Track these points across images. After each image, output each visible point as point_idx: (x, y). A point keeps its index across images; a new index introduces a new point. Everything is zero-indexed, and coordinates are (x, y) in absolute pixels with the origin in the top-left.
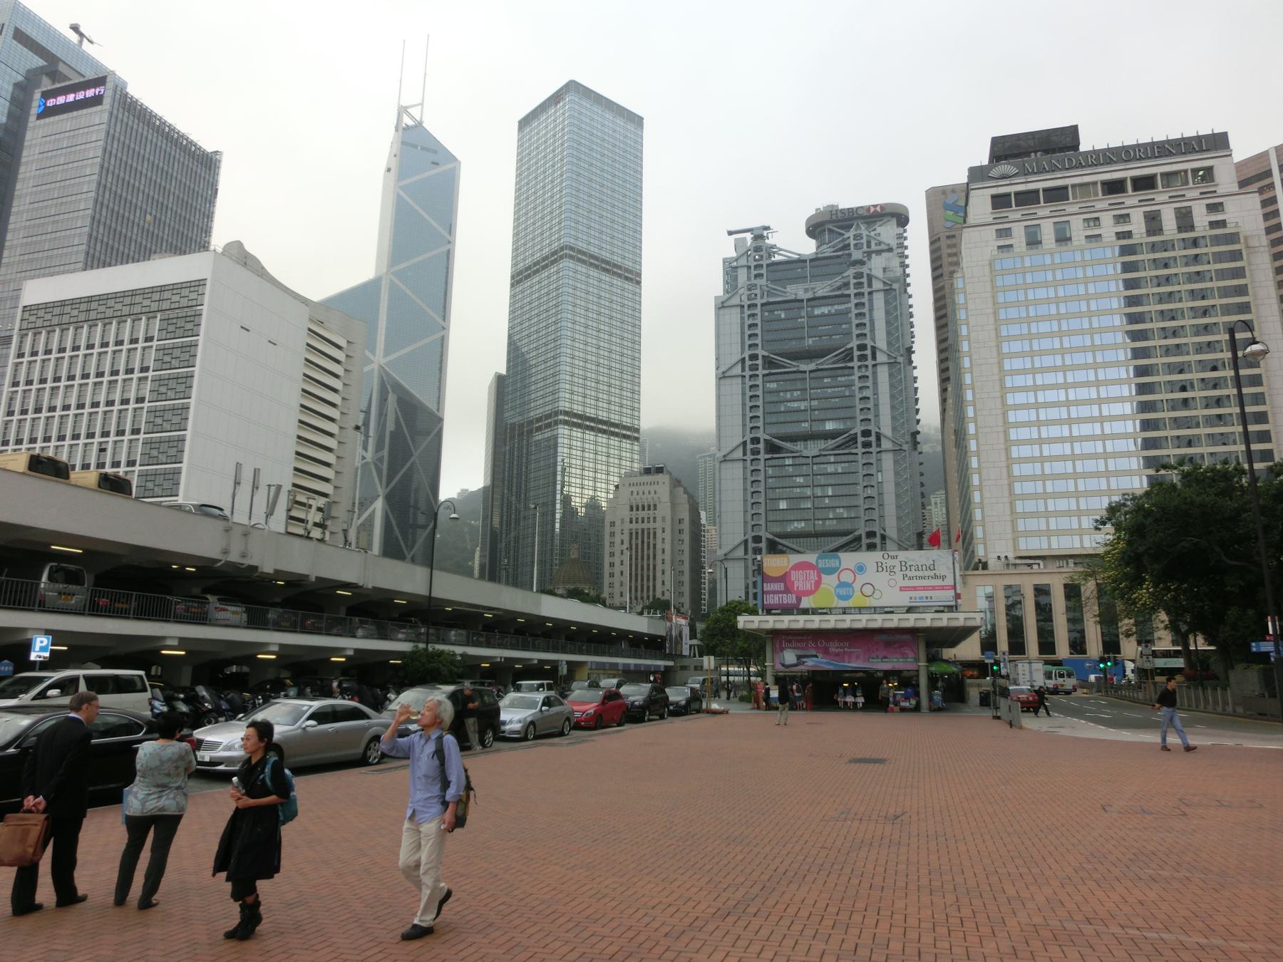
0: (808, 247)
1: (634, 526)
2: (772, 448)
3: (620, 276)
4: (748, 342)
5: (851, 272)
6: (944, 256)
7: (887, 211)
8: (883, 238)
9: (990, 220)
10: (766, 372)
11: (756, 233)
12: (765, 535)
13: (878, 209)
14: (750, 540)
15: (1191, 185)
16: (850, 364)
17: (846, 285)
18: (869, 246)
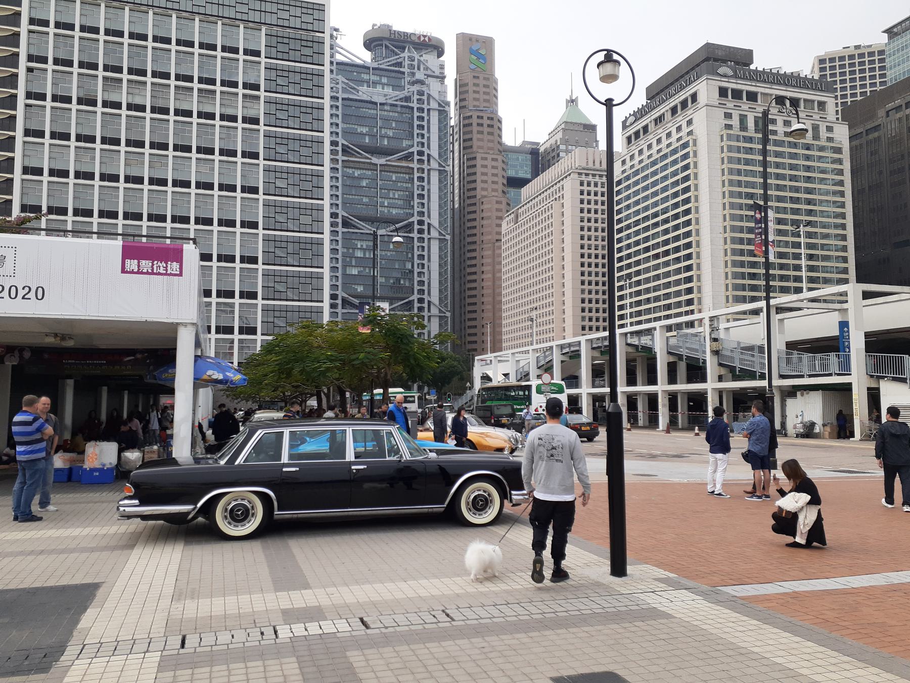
0: (366, 56)
2: (346, 224)
5: (415, 88)
6: (471, 91)
8: (429, 65)
9: (717, 104)
10: (345, 158)
13: (427, 39)
15: (816, 110)
16: (411, 165)
17: (407, 99)
18: (419, 69)
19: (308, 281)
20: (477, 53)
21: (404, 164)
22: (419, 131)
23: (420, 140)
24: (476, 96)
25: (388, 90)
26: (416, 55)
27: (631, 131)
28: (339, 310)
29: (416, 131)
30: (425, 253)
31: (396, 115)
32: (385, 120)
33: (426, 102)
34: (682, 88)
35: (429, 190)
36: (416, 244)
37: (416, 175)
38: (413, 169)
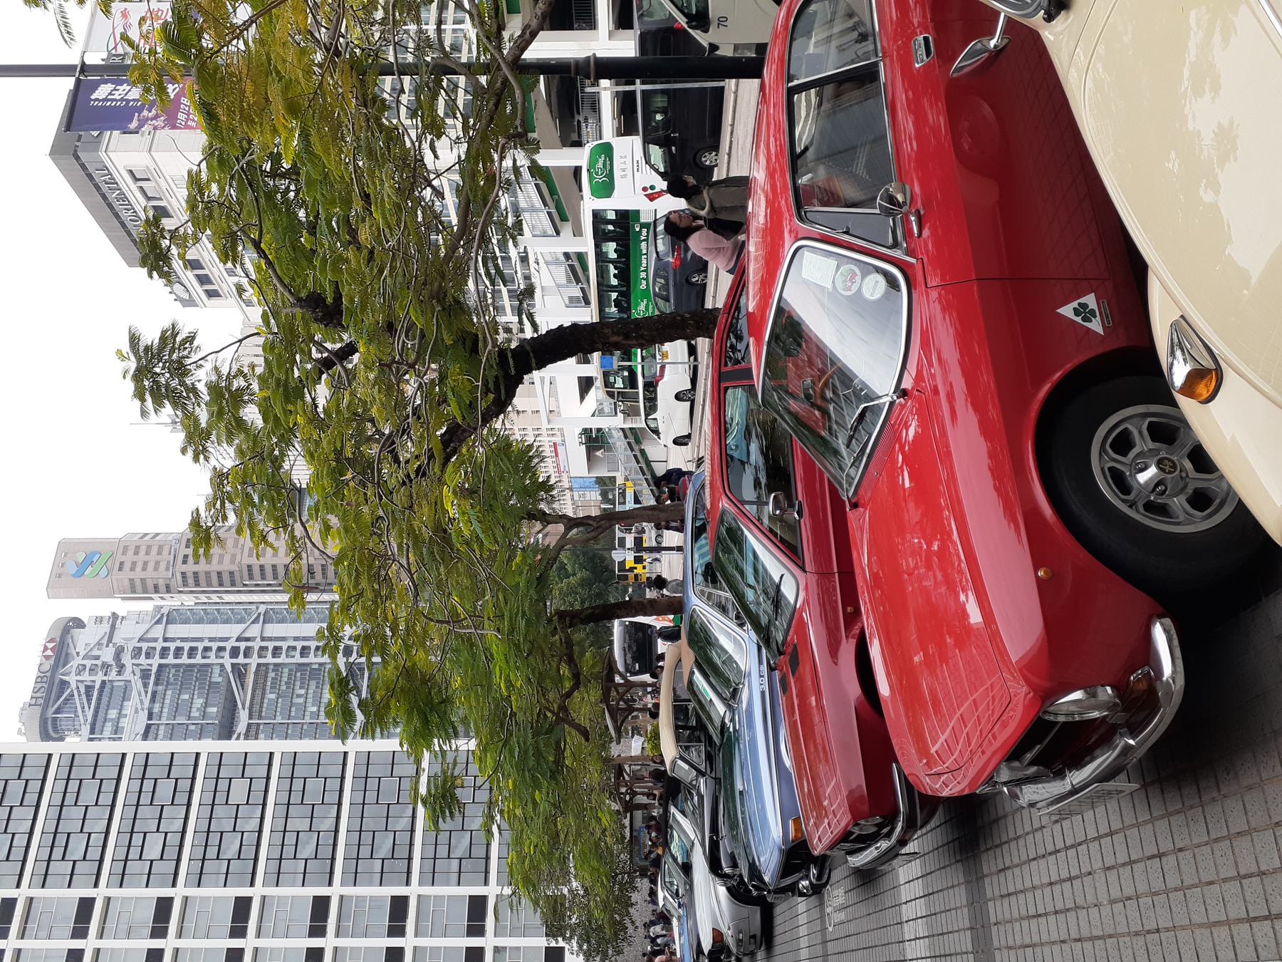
5: (127, 659)
6: (143, 575)
7: (57, 635)
8: (93, 641)
13: (50, 645)
16: (253, 668)
17: (145, 675)
18: (97, 658)
19: (373, 784)
20: (80, 565)
21: (250, 680)
22: (199, 656)
23: (212, 654)
24: (151, 566)
25: (129, 707)
26: (75, 663)
27: (198, 290)
29: (198, 660)
31: (169, 692)
32: (176, 711)
34: (122, 197)
35: (296, 639)
37: (269, 659)
38: (259, 665)
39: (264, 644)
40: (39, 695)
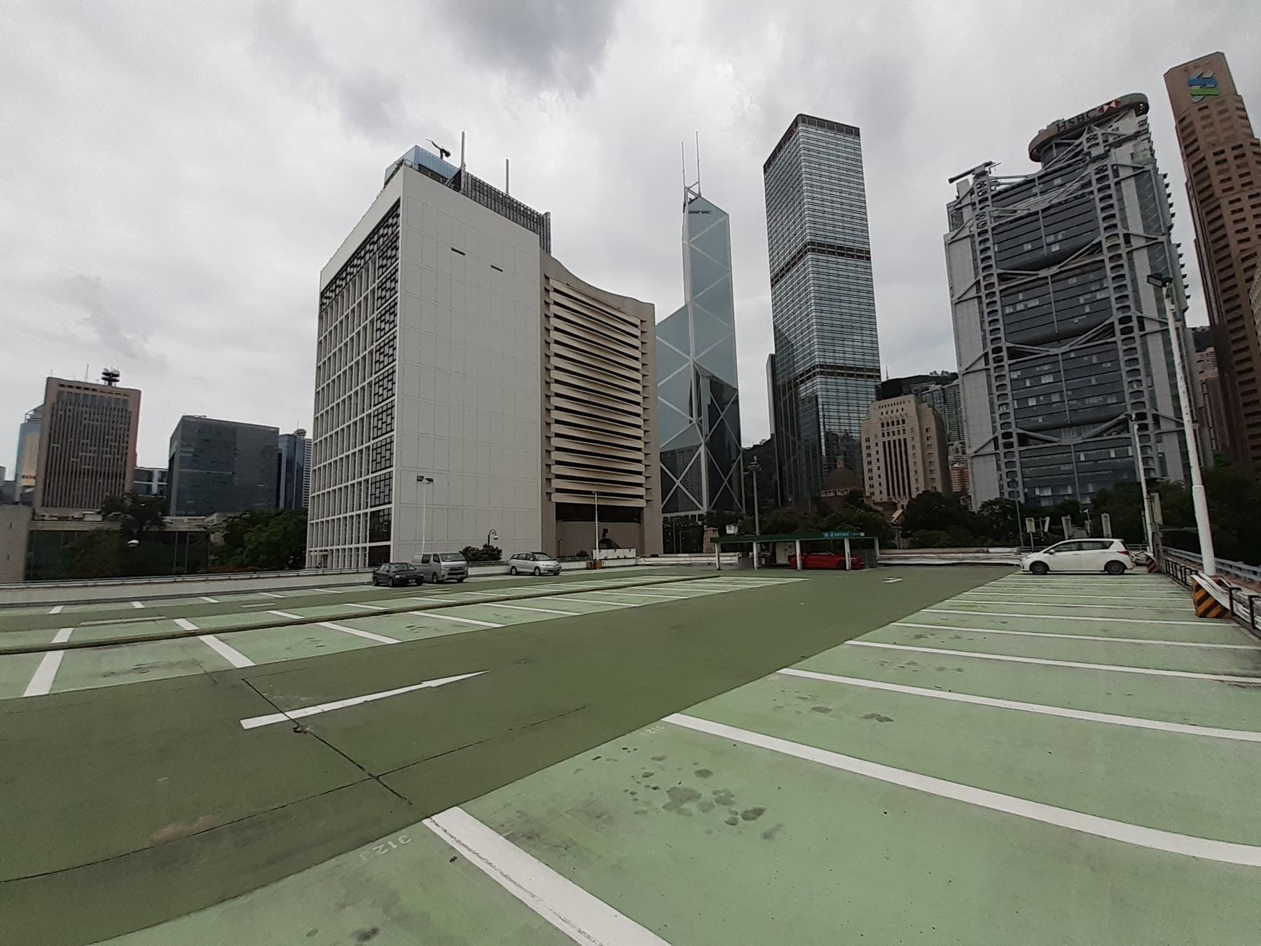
1: (886, 439)
2: (1013, 353)
3: (852, 256)
4: (981, 266)
5: (1092, 169)
11: (977, 171)
12: (1014, 430)
13: (1113, 105)
14: (1000, 437)
26: (1099, 131)
28: (1016, 448)
30: (1139, 355)
33: (1111, 176)
36: (1121, 347)
37: (1108, 265)
39: (1124, 256)
40: (1068, 126)
